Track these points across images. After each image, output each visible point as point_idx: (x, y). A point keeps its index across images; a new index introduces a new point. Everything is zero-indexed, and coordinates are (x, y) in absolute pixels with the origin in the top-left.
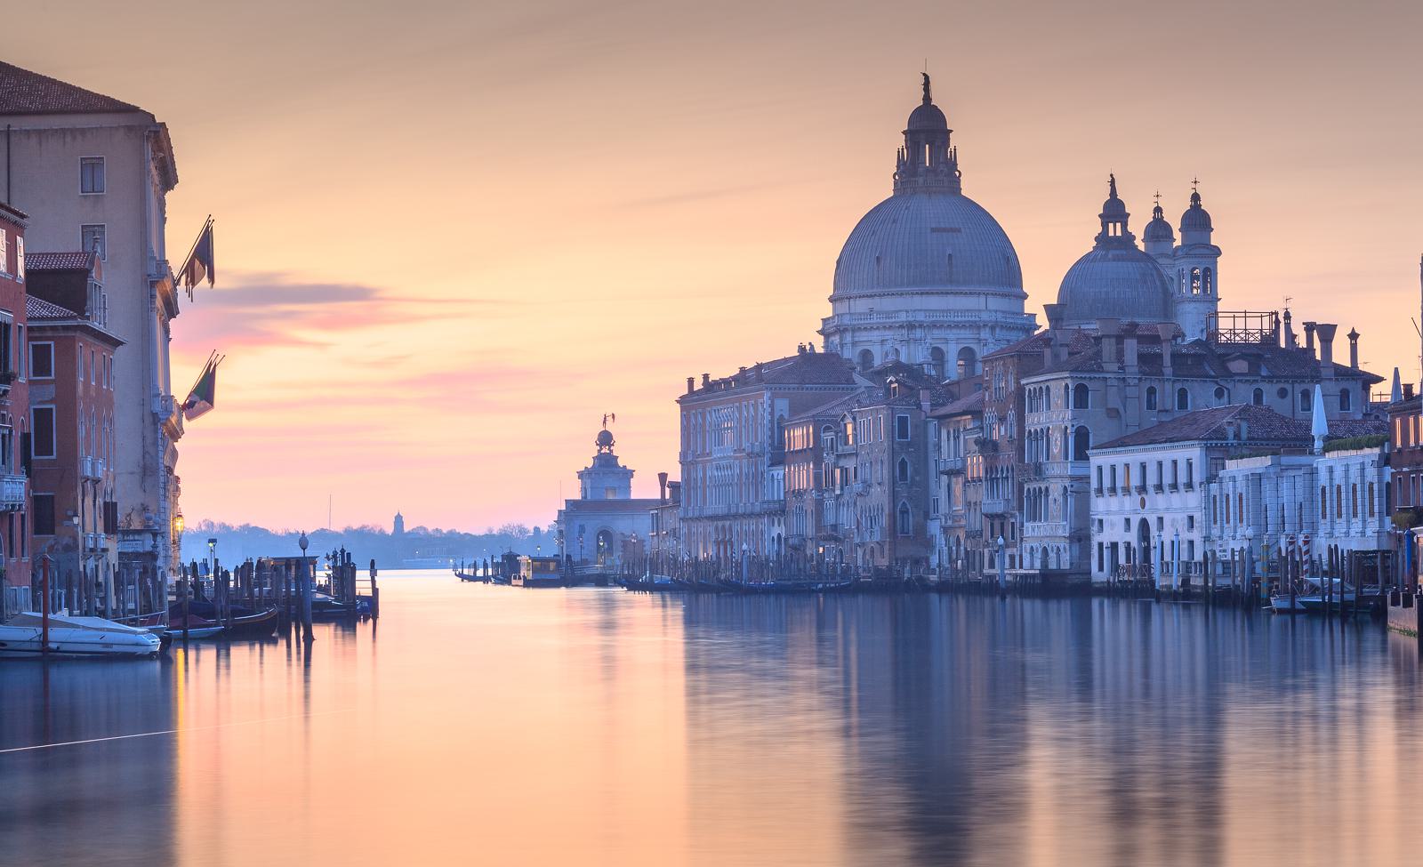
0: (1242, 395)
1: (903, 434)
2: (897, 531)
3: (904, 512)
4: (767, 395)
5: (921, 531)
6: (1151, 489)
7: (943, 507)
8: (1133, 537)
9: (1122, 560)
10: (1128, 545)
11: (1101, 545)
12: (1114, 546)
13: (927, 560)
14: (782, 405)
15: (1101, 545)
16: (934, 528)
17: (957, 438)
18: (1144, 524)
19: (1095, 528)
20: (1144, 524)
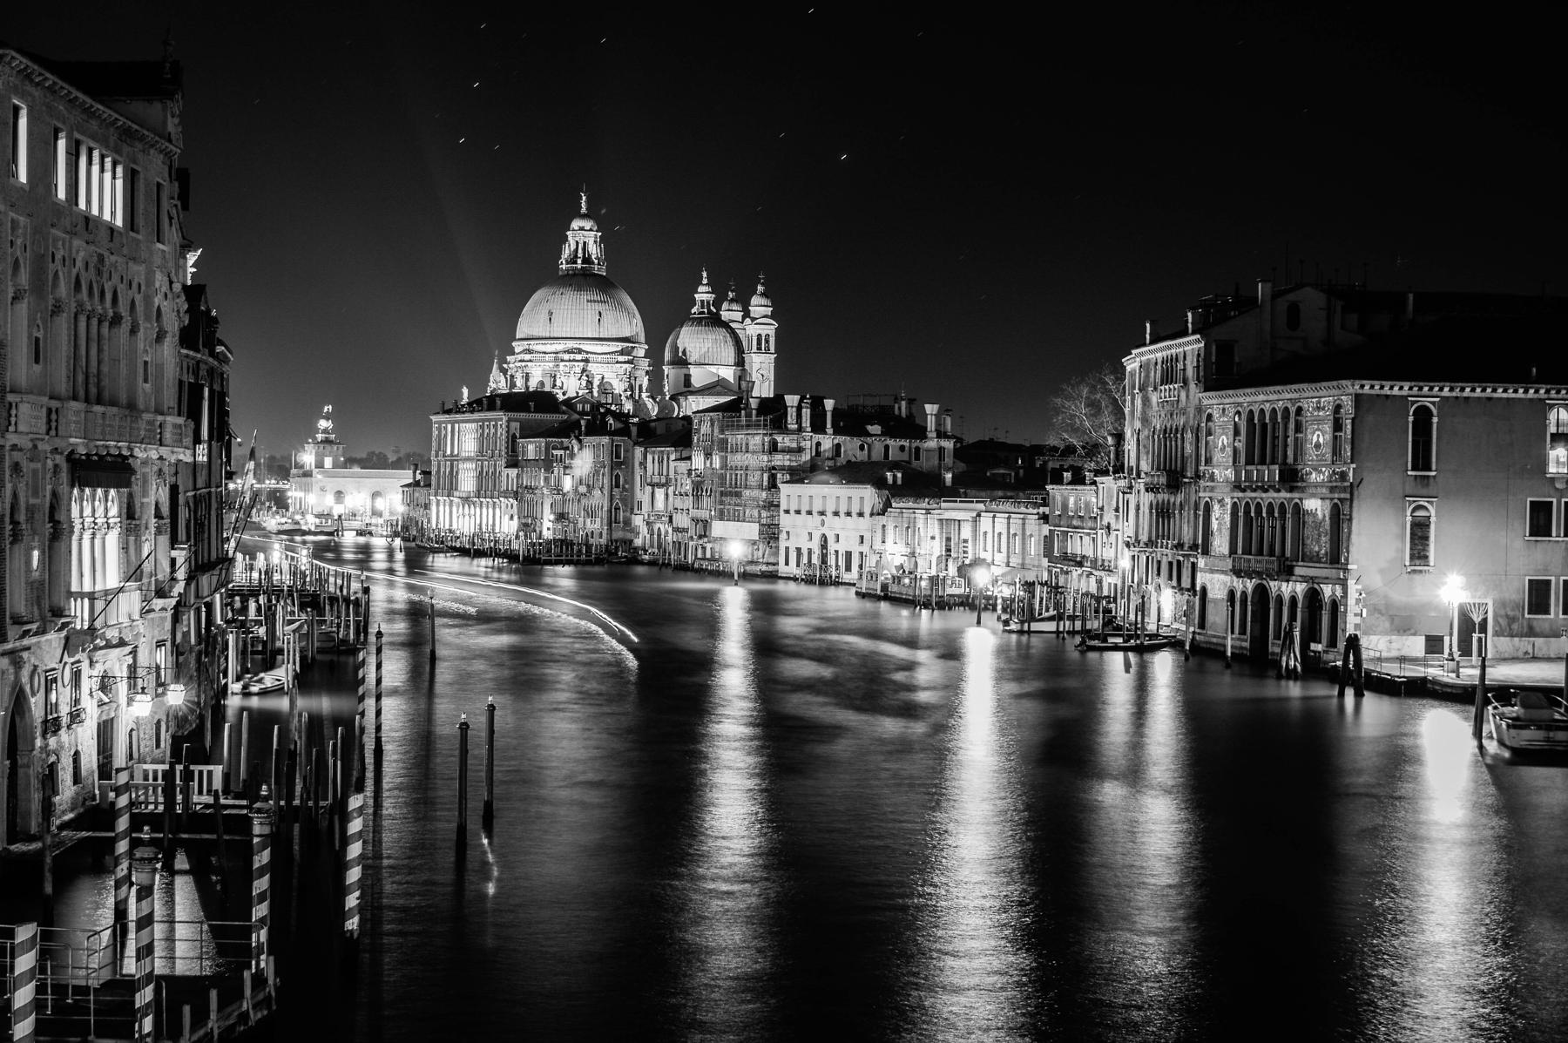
0: (878, 447)
1: (618, 456)
2: (612, 521)
3: (617, 509)
4: (505, 419)
5: (627, 522)
6: (829, 514)
7: (646, 507)
8: (815, 546)
9: (805, 560)
10: (810, 552)
11: (787, 549)
12: (799, 550)
13: (631, 541)
14: (515, 426)
15: (787, 549)
16: (638, 521)
17: (661, 462)
18: (824, 538)
19: (783, 536)
20: (824, 538)
